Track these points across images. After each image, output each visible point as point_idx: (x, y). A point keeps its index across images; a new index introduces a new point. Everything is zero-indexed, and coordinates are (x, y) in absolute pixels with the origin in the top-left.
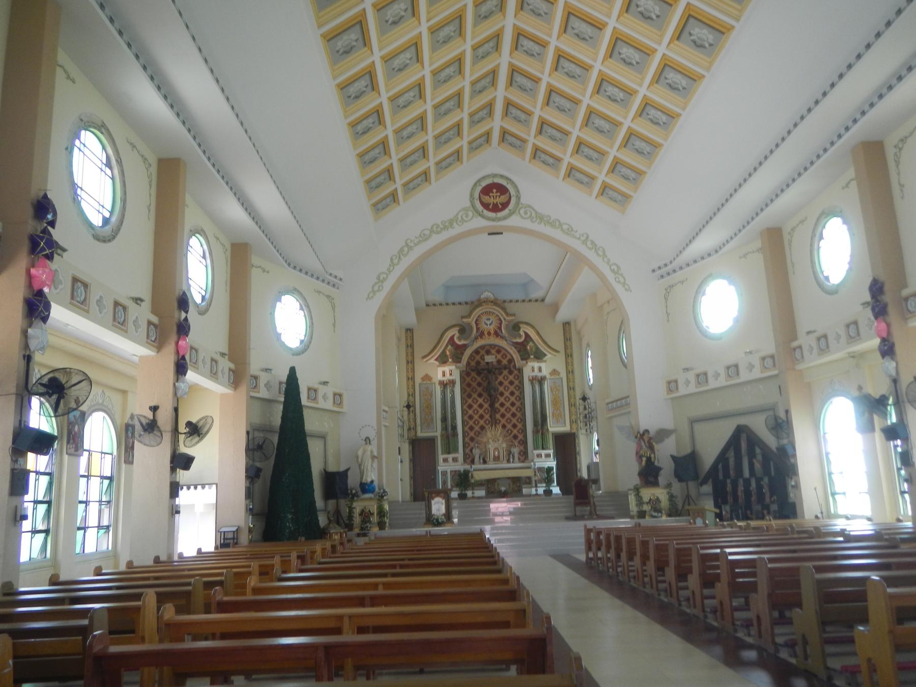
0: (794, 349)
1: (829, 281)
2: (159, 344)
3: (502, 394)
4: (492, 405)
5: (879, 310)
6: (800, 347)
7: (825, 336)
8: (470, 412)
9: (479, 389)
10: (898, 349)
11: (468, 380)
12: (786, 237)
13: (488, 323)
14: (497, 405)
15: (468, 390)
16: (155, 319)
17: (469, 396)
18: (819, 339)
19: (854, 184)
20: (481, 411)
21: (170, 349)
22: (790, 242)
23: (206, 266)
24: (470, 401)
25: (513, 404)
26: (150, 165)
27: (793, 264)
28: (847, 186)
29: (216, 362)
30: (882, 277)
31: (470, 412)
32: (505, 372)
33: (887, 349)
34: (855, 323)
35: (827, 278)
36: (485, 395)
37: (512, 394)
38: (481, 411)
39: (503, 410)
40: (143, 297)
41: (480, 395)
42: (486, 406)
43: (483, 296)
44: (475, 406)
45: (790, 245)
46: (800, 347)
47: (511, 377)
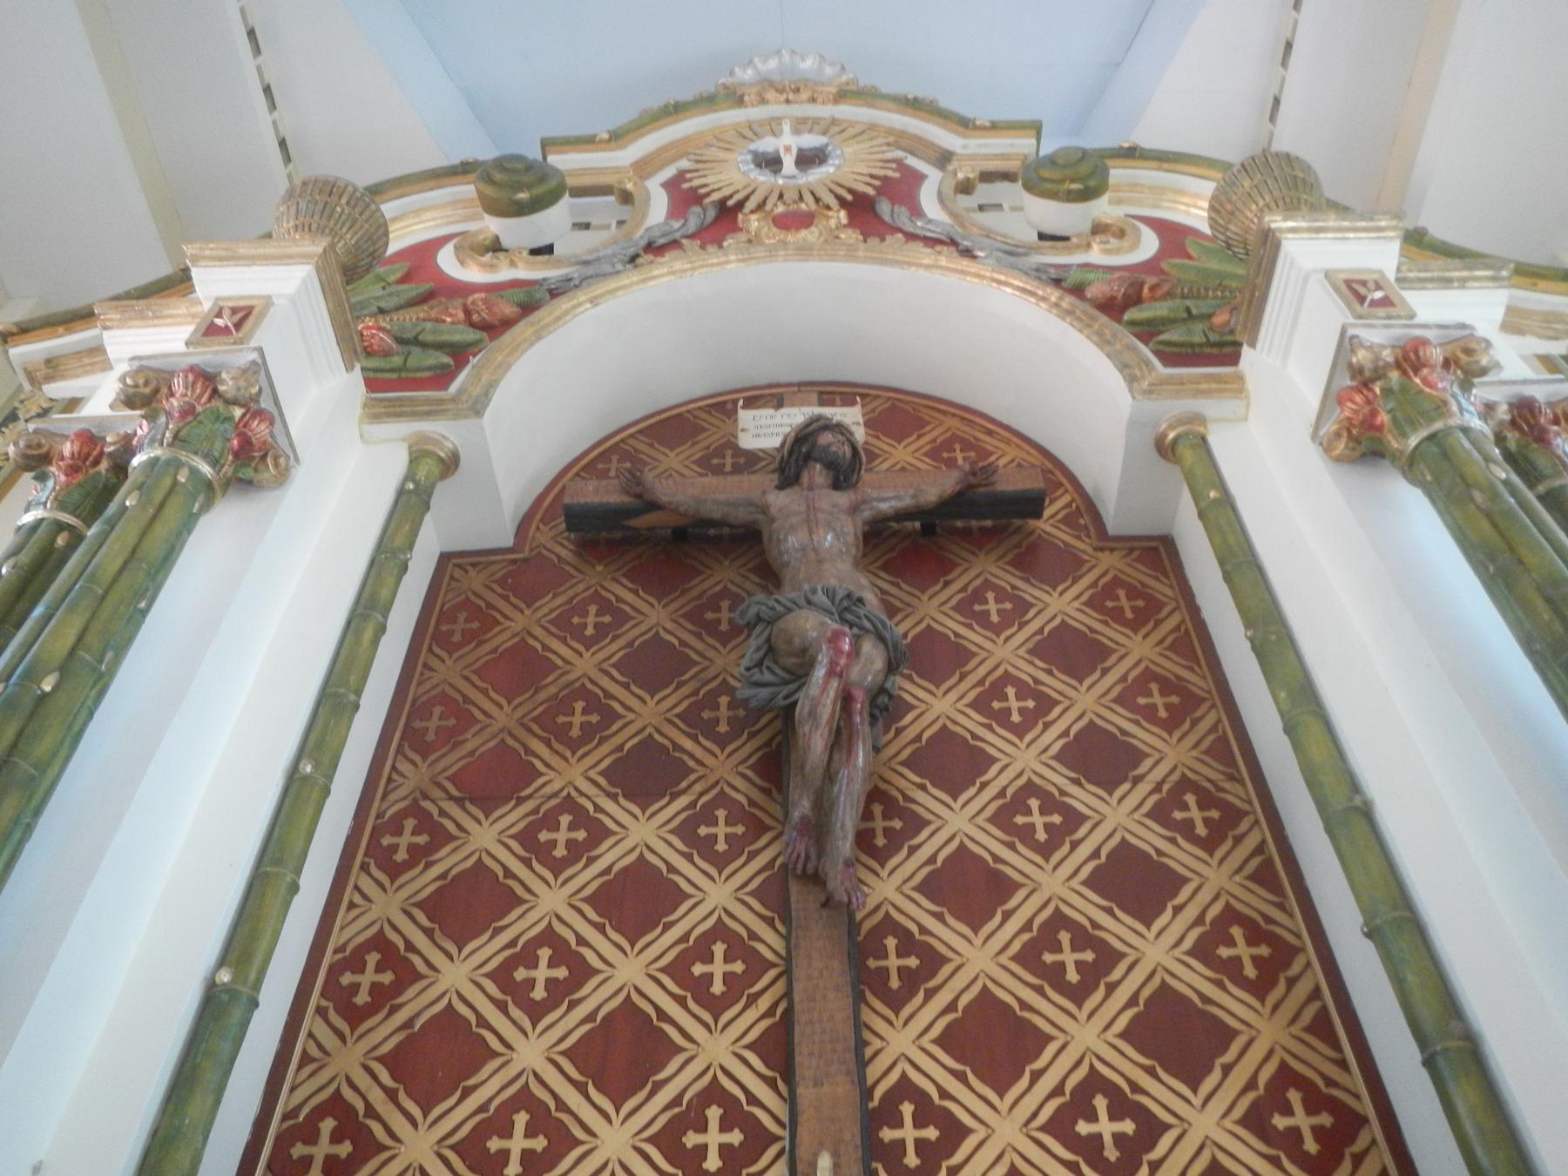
3: (953, 762)
4: (798, 886)
8: (457, 976)
9: (647, 714)
11: (523, 622)
13: (787, 143)
14: (891, 889)
15: (501, 715)
17: (495, 781)
20: (628, 971)
24: (487, 838)
25: (1135, 883)
31: (457, 976)
32: (986, 568)
36: (725, 769)
37: (1098, 757)
38: (628, 971)
39: (979, 959)
41: (645, 775)
42: (717, 896)
43: (748, 75)
44: (552, 901)
47: (1060, 605)
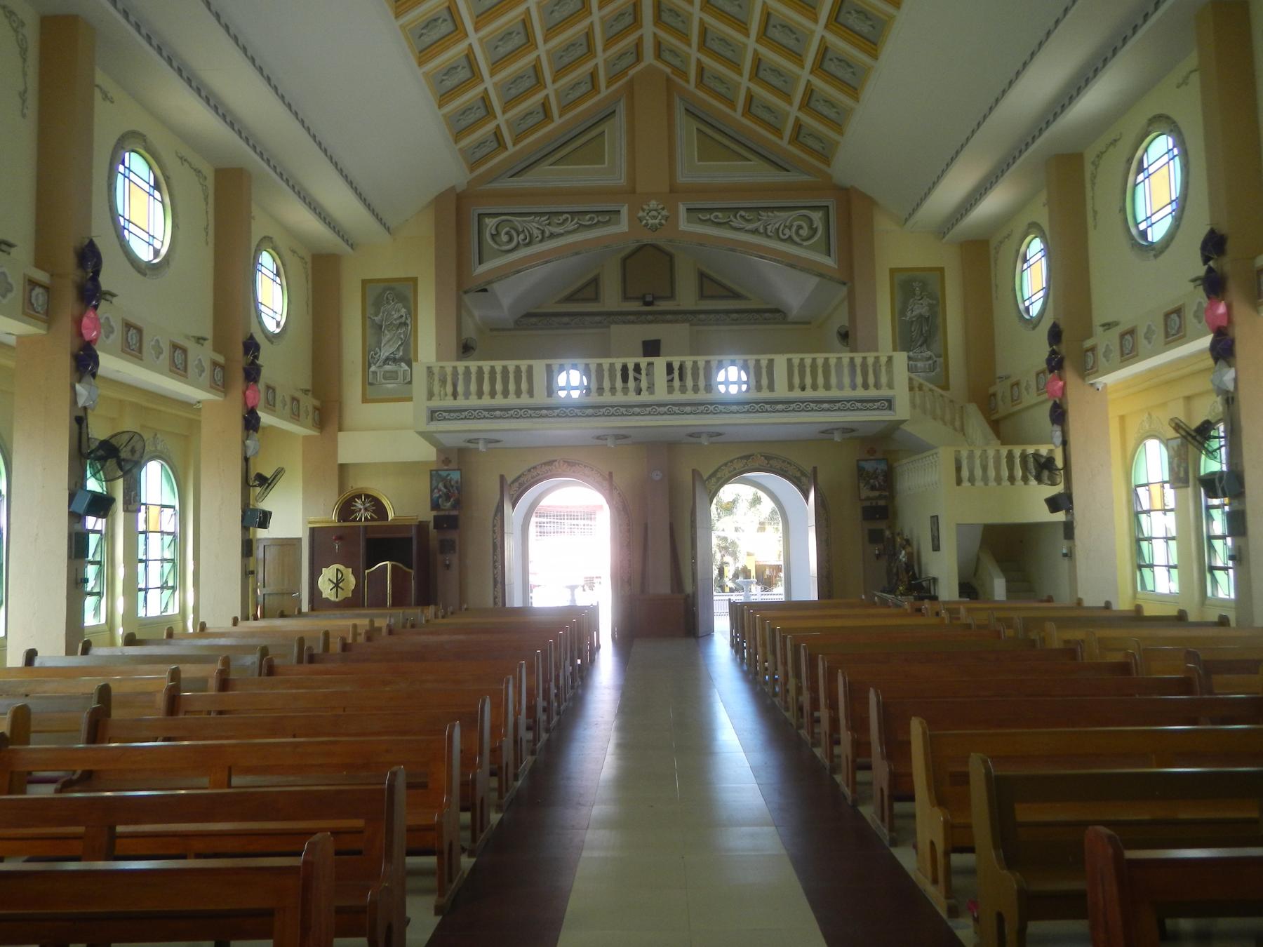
0: (1087, 351)
1: (1146, 239)
2: (48, 317)
5: (1214, 285)
6: (1093, 349)
7: (1132, 332)
10: (1239, 349)
12: (1089, 168)
16: (41, 276)
18: (1122, 336)
19: (1195, 79)
21: (65, 324)
22: (1094, 177)
23: (162, 202)
26: (23, 24)
27: (1095, 212)
28: (1185, 82)
29: (184, 351)
30: (1223, 229)
33: (1223, 350)
34: (1178, 311)
35: (1144, 234)
40: (10, 240)
45: (1093, 184)
46: (1093, 349)
